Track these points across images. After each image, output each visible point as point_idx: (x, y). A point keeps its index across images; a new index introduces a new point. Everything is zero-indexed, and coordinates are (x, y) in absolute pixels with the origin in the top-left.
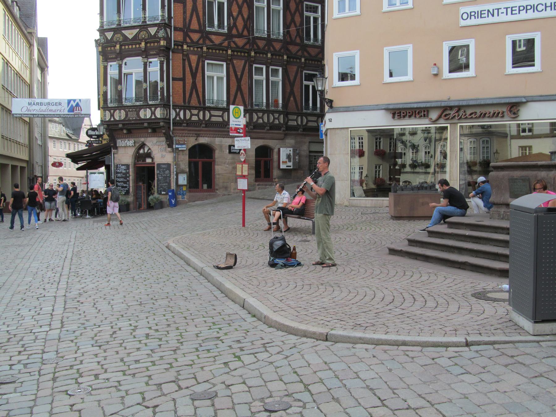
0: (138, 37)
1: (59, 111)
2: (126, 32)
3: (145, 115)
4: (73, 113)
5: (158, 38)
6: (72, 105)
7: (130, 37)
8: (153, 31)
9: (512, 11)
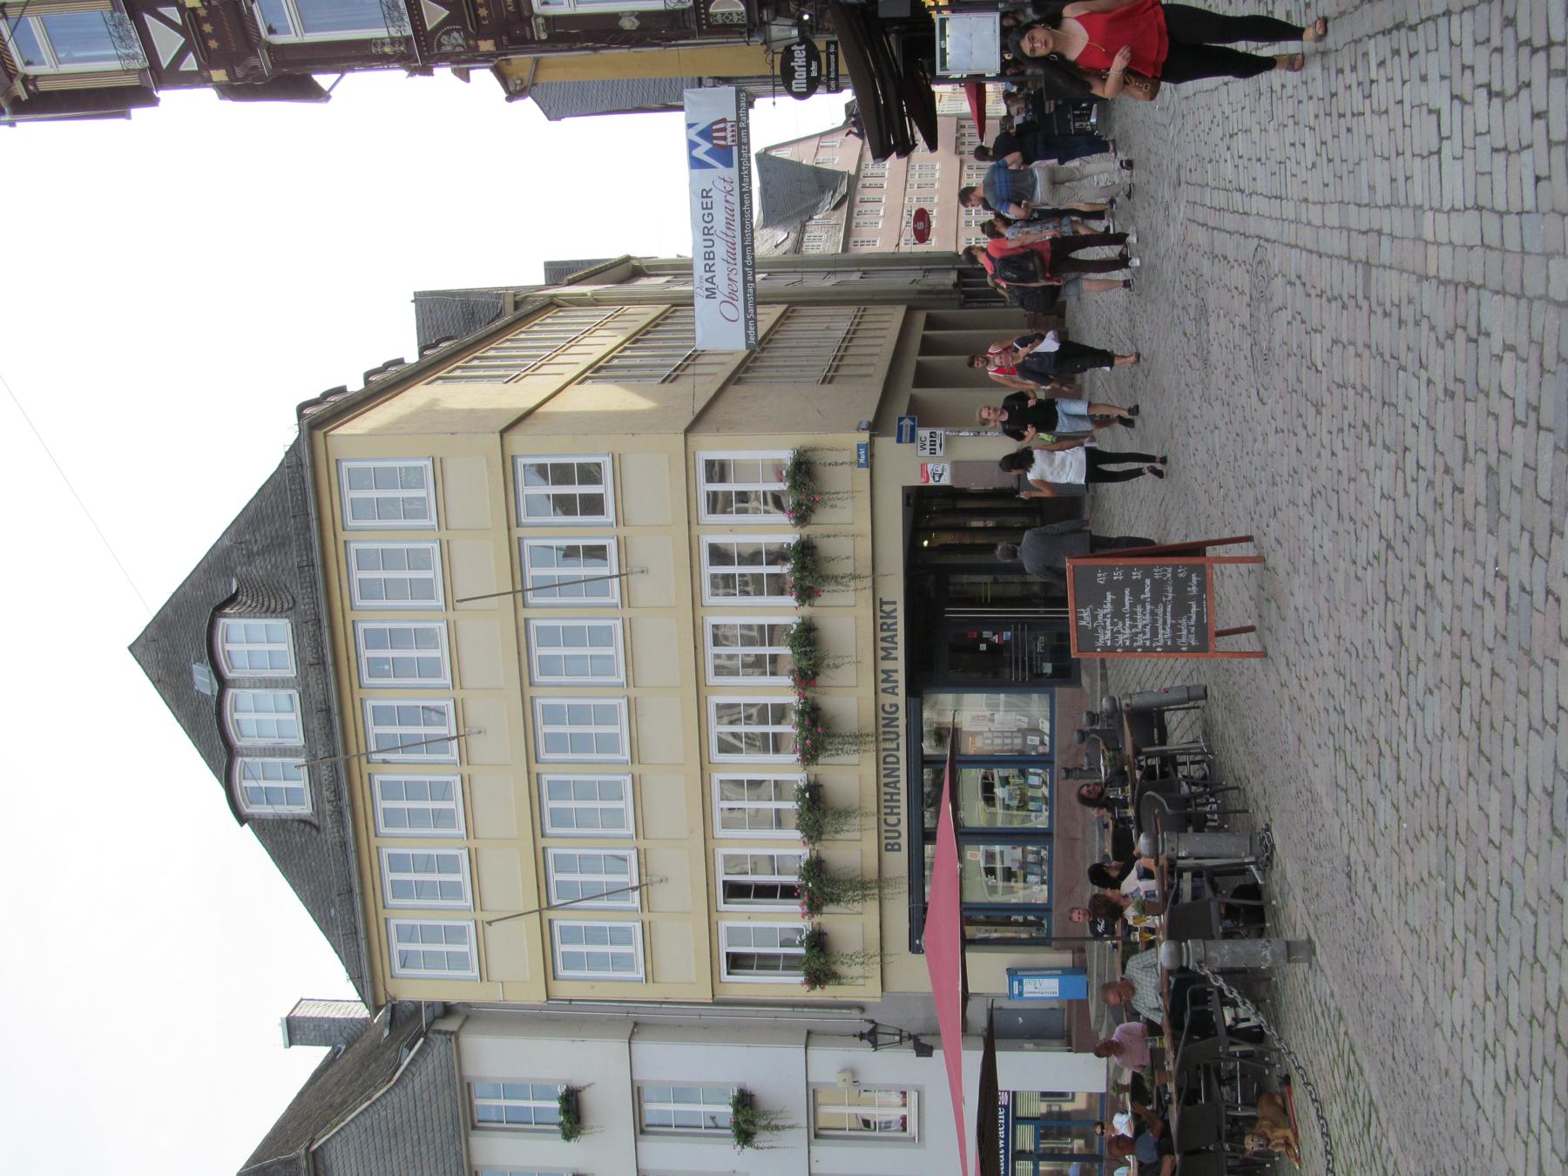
1: (729, 198)
4: (735, 150)
6: (708, 153)
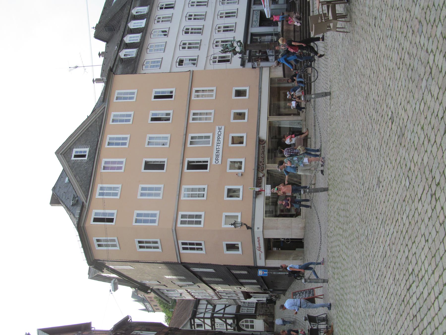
9: (218, 143)
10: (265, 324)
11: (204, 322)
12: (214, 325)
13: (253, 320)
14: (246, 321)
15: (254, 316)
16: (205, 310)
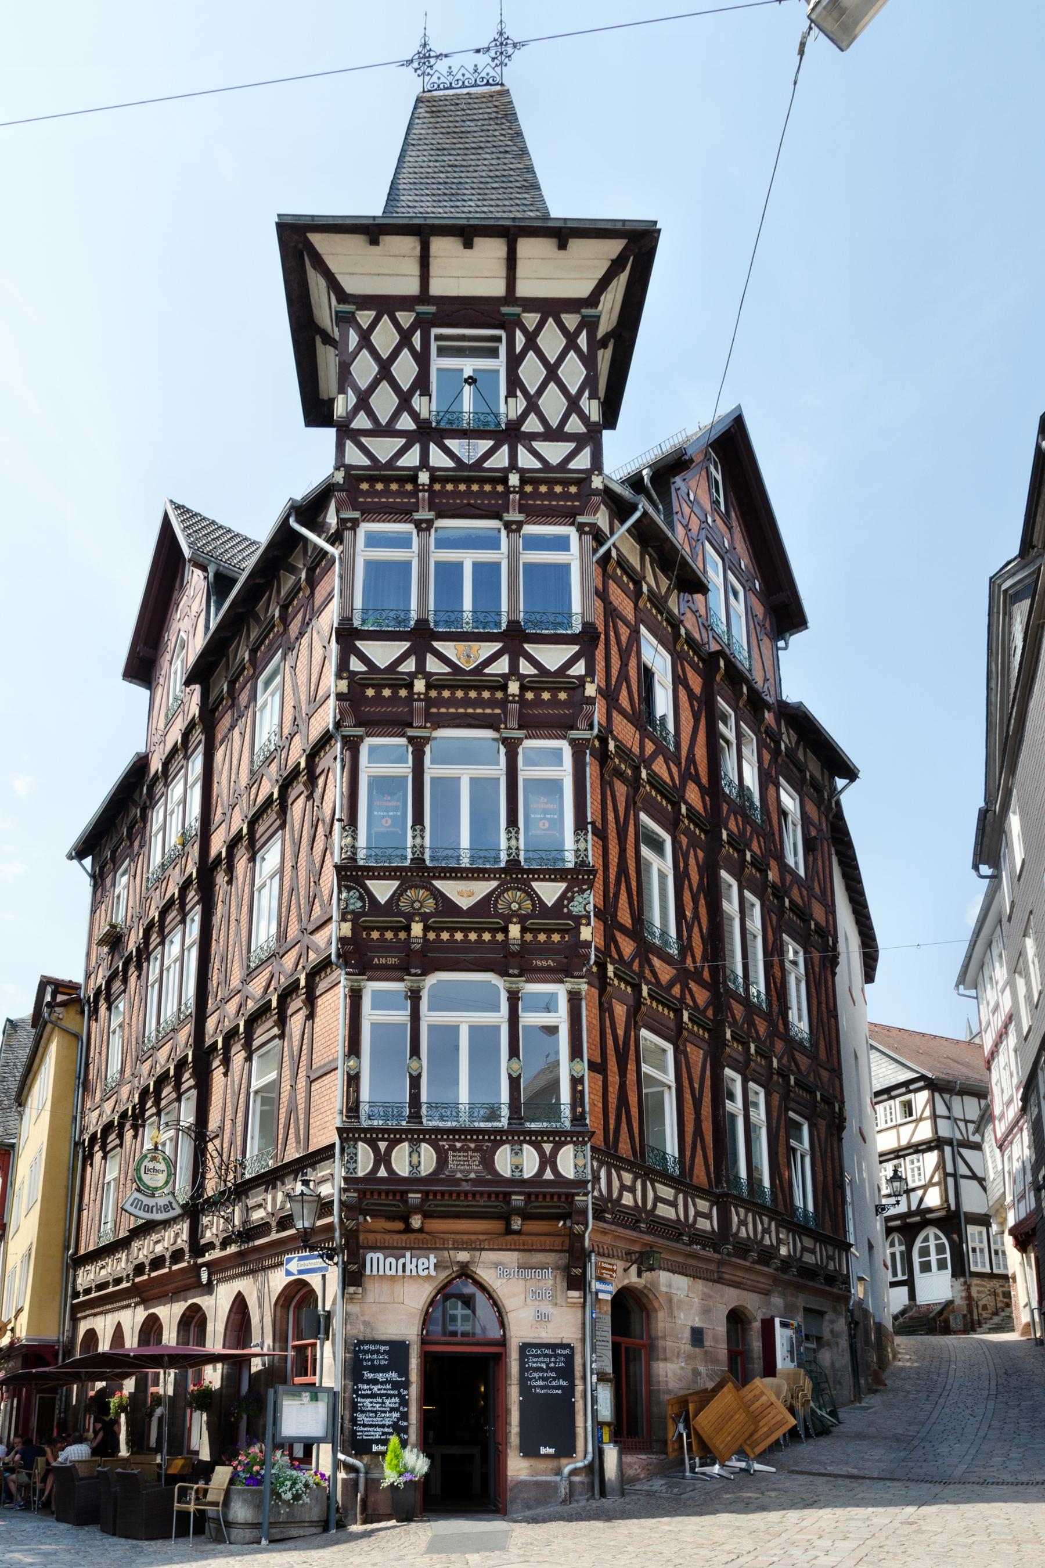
0: (495, 906)
2: (449, 888)
3: (518, 1168)
5: (570, 916)
7: (465, 903)
8: (550, 892)
10: (939, 1308)
11: (921, 1119)
12: (917, 1152)
13: (946, 1268)
14: (940, 1249)
15: (960, 1268)
16: (961, 1120)
